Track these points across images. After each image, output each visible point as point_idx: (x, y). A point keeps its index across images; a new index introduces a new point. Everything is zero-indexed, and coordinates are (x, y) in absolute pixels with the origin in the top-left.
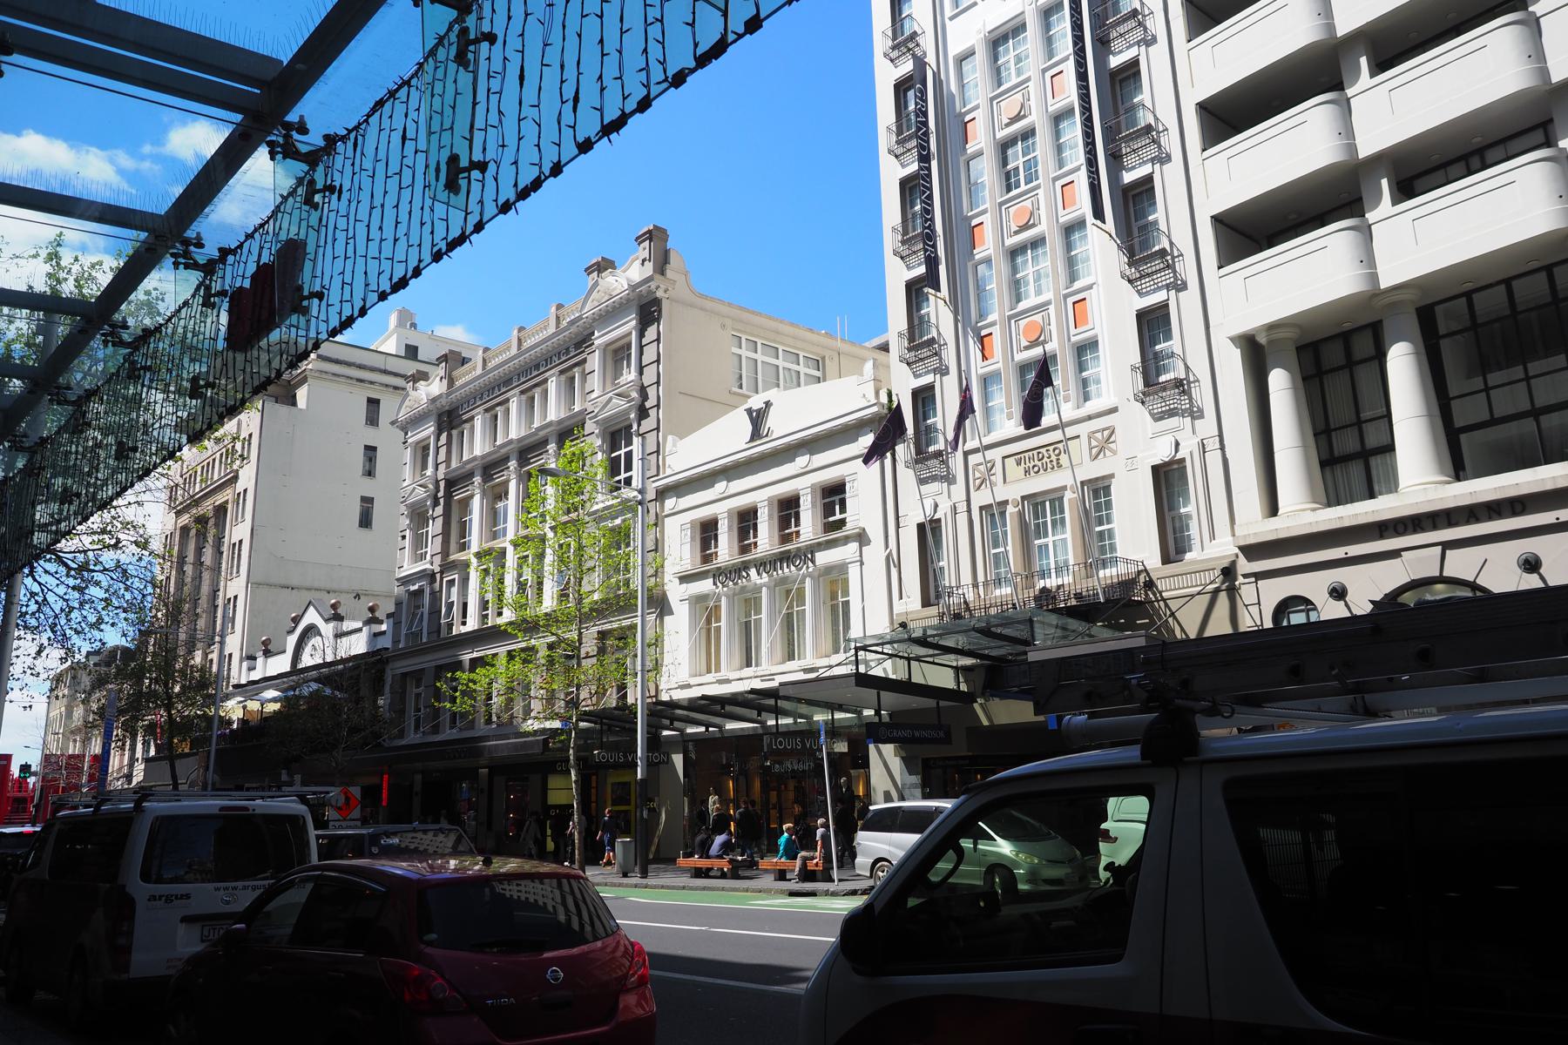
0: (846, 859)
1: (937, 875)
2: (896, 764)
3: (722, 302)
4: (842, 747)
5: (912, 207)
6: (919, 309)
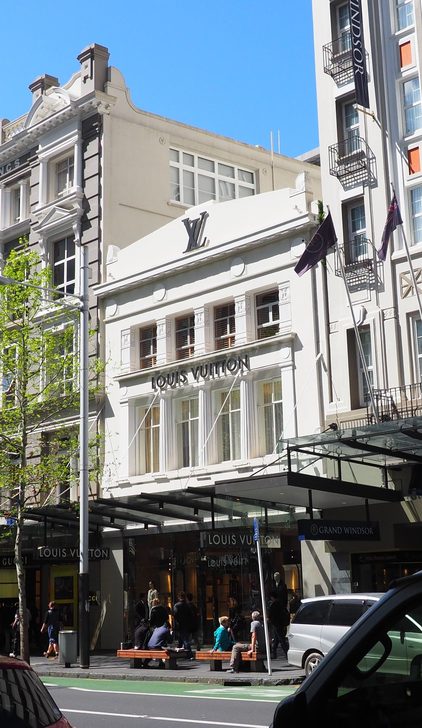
0: (279, 650)
1: (366, 665)
2: (327, 559)
3: (160, 118)
4: (275, 543)
5: (342, 26)
6: (349, 124)
